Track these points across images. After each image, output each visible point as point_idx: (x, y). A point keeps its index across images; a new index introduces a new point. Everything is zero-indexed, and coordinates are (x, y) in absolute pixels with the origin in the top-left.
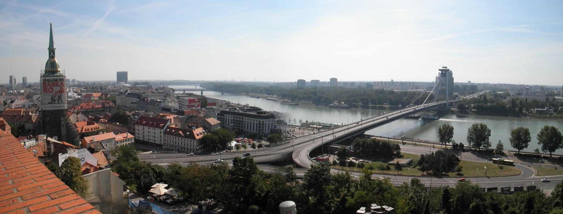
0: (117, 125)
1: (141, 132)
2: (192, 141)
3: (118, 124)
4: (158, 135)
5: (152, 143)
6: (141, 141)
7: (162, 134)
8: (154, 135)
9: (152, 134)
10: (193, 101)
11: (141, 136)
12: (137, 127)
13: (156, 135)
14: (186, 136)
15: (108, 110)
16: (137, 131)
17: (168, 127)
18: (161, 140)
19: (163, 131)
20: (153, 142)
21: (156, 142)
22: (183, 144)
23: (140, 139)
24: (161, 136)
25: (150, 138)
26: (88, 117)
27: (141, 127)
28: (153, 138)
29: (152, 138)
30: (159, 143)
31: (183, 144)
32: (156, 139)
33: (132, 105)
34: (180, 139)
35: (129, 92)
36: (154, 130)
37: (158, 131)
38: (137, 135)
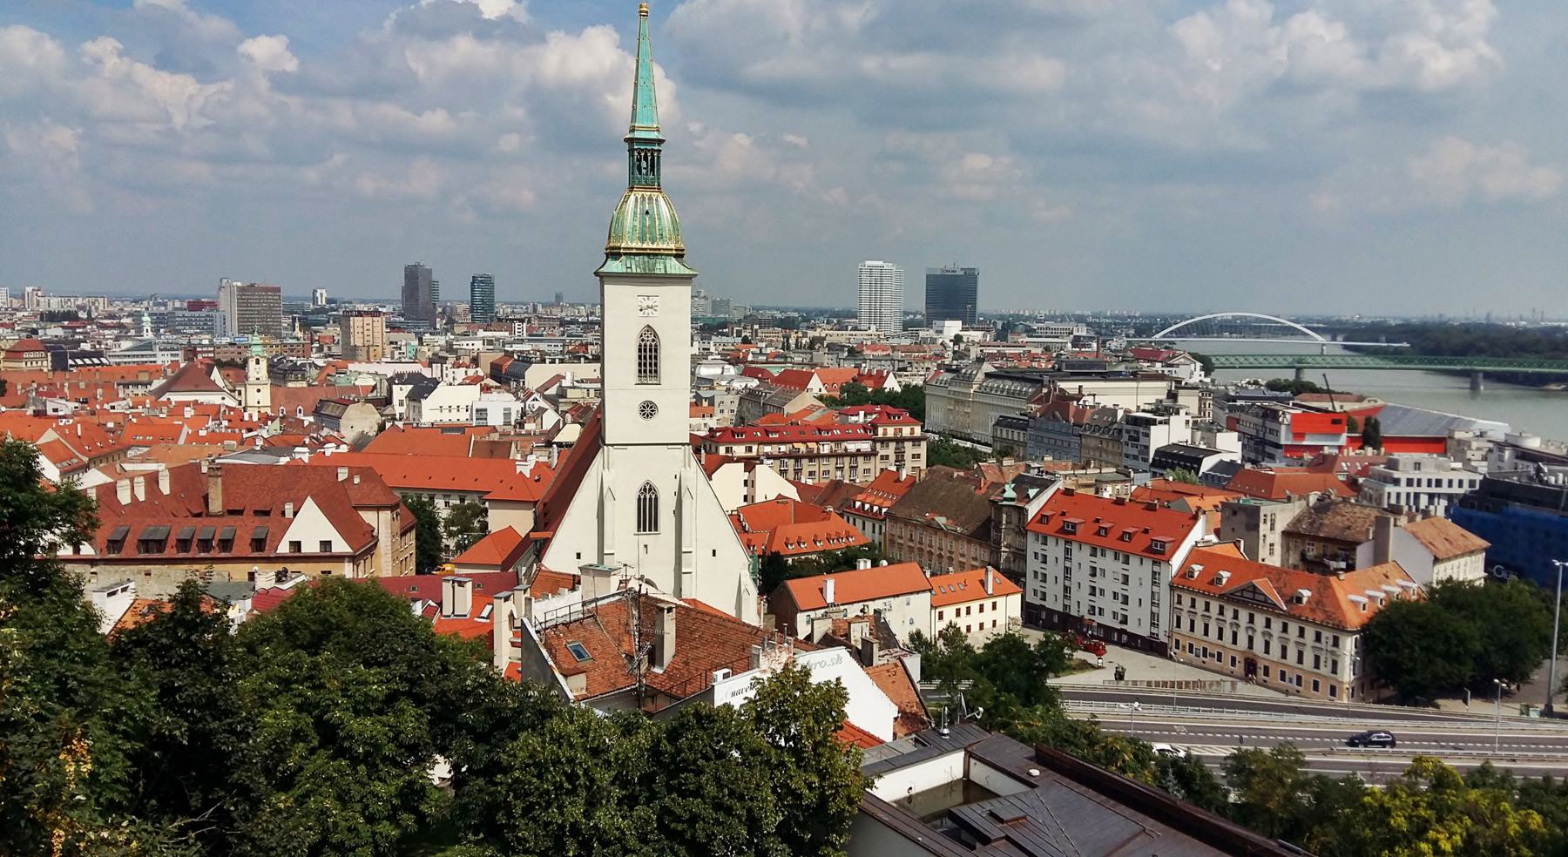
1: (1054, 570)
2: (1327, 635)
3: (941, 520)
4: (1139, 589)
6: (1051, 612)
8: (1118, 587)
9: (1109, 584)
12: (1033, 546)
13: (1133, 591)
15: (891, 450)
16: (1032, 565)
17: (1196, 554)
21: (1131, 627)
23: (1049, 604)
25: (1099, 602)
26: (796, 483)
27: (1055, 550)
28: (1117, 606)
29: (1109, 604)
30: (1144, 631)
32: (1133, 611)
33: (1004, 433)
34: (1260, 620)
35: (987, 367)
36: (1119, 565)
37: (1140, 570)
38: (1032, 583)
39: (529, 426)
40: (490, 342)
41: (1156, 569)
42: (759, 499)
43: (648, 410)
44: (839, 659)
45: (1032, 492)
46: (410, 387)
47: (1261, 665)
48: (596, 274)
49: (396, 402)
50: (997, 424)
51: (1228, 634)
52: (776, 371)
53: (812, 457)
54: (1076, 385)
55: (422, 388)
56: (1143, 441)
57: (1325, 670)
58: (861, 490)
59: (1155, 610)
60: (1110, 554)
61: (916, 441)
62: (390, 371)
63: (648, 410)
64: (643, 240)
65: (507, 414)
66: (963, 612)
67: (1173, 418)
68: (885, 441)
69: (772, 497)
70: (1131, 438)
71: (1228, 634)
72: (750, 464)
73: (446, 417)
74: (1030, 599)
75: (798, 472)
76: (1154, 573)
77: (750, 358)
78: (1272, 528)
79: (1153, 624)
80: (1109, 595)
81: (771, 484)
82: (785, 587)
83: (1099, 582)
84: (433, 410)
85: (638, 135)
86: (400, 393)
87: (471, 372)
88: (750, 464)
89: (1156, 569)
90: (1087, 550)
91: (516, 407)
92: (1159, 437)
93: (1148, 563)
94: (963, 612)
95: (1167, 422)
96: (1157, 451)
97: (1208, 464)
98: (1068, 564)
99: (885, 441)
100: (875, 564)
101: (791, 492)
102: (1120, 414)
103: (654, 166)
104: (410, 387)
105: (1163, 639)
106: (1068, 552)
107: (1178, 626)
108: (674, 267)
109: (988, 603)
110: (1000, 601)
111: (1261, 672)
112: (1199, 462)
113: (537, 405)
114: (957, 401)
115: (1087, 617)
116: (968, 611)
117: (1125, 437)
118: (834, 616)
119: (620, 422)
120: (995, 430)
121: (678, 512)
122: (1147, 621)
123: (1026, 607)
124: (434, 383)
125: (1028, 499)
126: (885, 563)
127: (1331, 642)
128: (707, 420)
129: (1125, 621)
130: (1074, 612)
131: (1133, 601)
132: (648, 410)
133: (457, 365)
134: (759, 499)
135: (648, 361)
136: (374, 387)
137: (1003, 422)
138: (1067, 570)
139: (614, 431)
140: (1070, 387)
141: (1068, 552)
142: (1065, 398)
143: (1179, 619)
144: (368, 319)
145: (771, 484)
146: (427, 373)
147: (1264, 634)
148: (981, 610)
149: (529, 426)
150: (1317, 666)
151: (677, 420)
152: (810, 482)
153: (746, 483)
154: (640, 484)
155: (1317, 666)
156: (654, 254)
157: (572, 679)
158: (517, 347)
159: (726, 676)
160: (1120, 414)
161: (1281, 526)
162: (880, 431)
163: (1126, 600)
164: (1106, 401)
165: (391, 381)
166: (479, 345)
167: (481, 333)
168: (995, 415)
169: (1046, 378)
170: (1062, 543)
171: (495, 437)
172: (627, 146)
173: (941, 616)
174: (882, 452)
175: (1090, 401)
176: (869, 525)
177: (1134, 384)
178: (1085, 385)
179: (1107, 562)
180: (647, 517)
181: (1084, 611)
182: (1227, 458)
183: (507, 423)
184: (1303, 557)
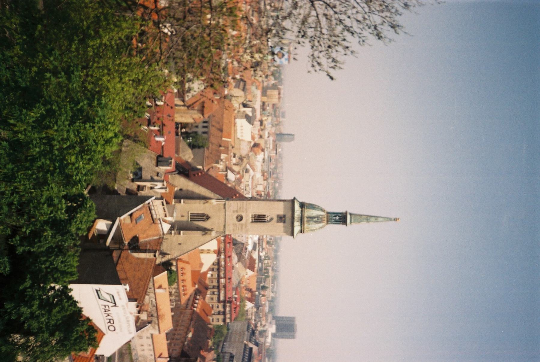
0: (187, 333)
3: (190, 335)
42: (202, 256)
44: (130, 333)
48: (295, 198)
50: (231, 354)
52: (255, 256)
58: (204, 299)
61: (224, 320)
68: (224, 307)
69: (203, 261)
82: (164, 271)
85: (349, 217)
99: (224, 307)
101: (204, 269)
103: (337, 222)
108: (297, 229)
134: (202, 256)
135: (259, 219)
139: (233, 205)
168: (234, 354)
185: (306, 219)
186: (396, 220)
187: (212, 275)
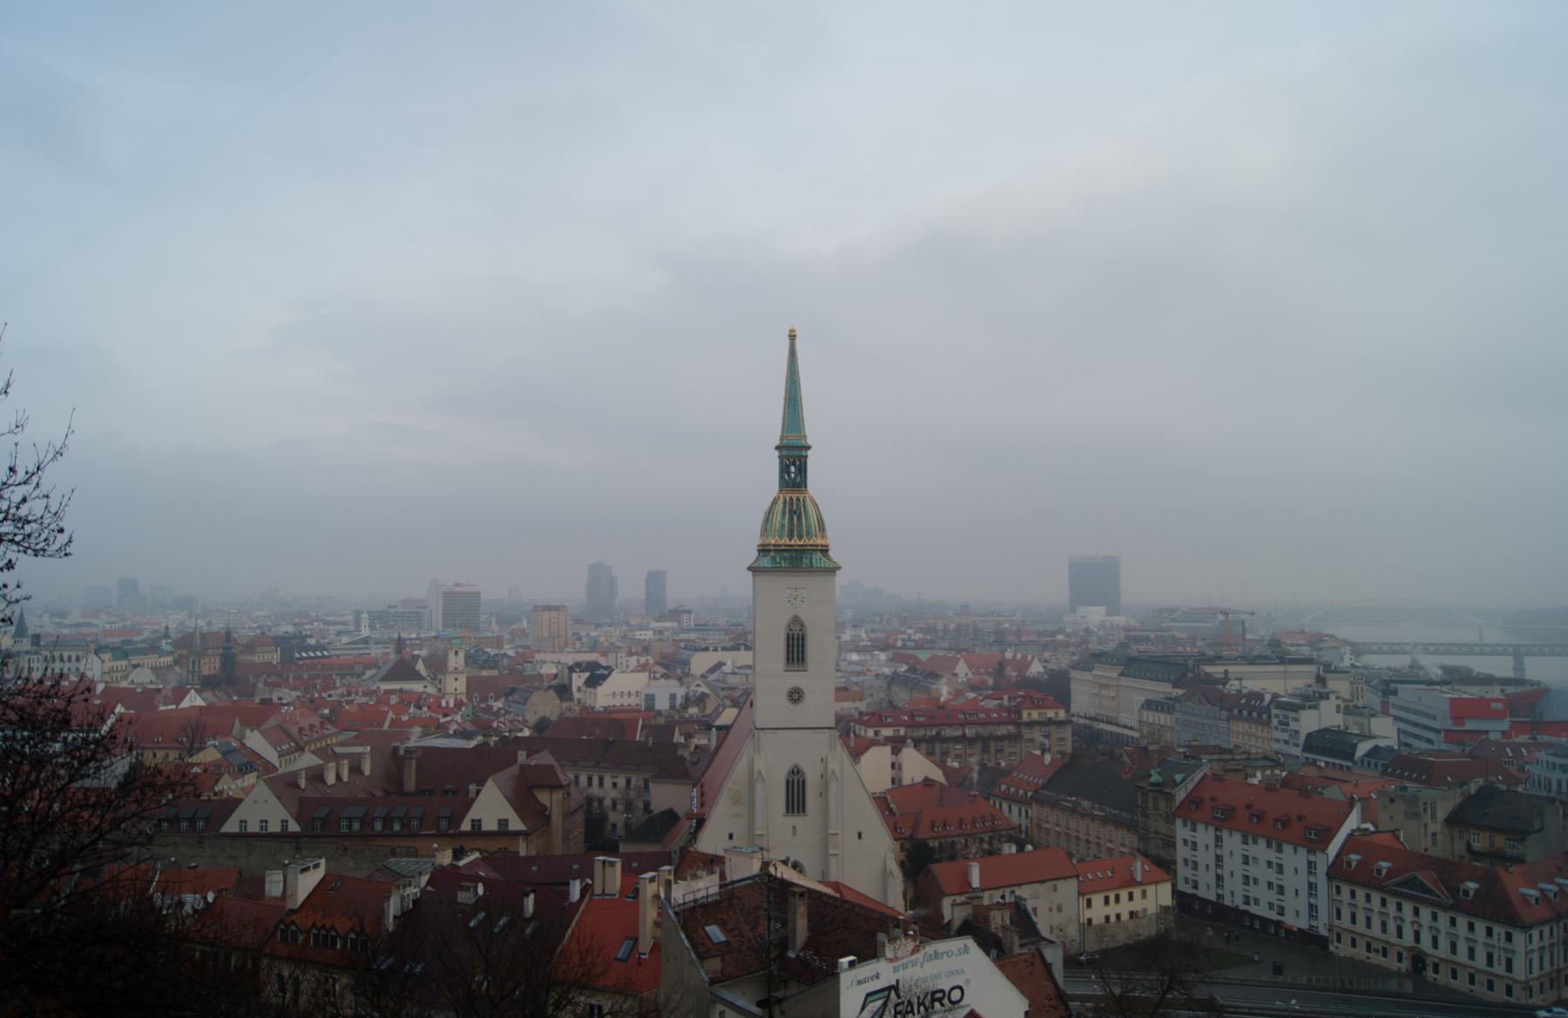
1: (1205, 857)
2: (1499, 930)
3: (1086, 804)
4: (1295, 880)
5: (1265, 922)
7: (1321, 880)
9: (1260, 871)
10: (1480, 708)
11: (1206, 879)
12: (1181, 832)
13: (1288, 880)
14: (1459, 905)
16: (1182, 852)
17: (1351, 843)
18: (1313, 908)
19: (1323, 861)
20: (1273, 916)
21: (1290, 920)
22: (1444, 942)
23: (1202, 893)
24: (1312, 887)
25: (1253, 892)
26: (942, 765)
27: (1205, 835)
28: (1273, 896)
30: (1302, 923)
31: (1444, 942)
33: (1150, 716)
34: (1425, 913)
37: (1295, 859)
38: (1182, 871)
39: (693, 710)
40: (661, 632)
41: (1312, 858)
42: (906, 781)
43: (796, 696)
44: (966, 949)
45: (1178, 777)
46: (587, 674)
47: (1429, 961)
48: (749, 568)
49: (574, 689)
51: (1392, 928)
53: (956, 740)
54: (1221, 669)
55: (597, 676)
56: (1293, 726)
57: (1499, 969)
59: (1313, 901)
60: (1262, 842)
62: (570, 659)
63: (796, 696)
64: (791, 537)
65: (673, 697)
66: (1112, 899)
67: (1323, 703)
69: (919, 779)
70: (1280, 722)
71: (1392, 928)
72: (897, 745)
73: (618, 702)
74: (1182, 887)
75: (945, 754)
76: (1310, 863)
77: (899, 644)
78: (1433, 817)
79: (1311, 916)
80: (1263, 884)
81: (917, 766)
83: (1253, 871)
84: (604, 697)
86: (578, 680)
87: (643, 660)
88: (897, 745)
89: (1312, 858)
90: (1237, 837)
91: (681, 692)
92: (1308, 722)
93: (1302, 852)
94: (1112, 899)
95: (1314, 707)
96: (1309, 736)
97: (1363, 748)
98: (1219, 852)
100: (1021, 849)
101: (937, 775)
102: (1268, 698)
104: (587, 674)
105: (1323, 932)
106: (1218, 839)
107: (1339, 917)
109: (1137, 892)
110: (1150, 889)
111: (1430, 969)
112: (1354, 746)
113: (700, 690)
114: (1102, 686)
115: (1243, 907)
116: (1117, 899)
117: (1275, 722)
118: (975, 902)
119: (770, 705)
120: (1140, 714)
121: (824, 794)
122: (1304, 911)
123: (1176, 893)
124: (610, 670)
125: (1175, 784)
126: (1029, 847)
127: (1503, 937)
128: (857, 704)
129: (1281, 911)
130: (1227, 902)
131: (1289, 891)
132: (796, 696)
133: (630, 654)
134: (906, 781)
136: (556, 676)
137: (1149, 705)
138: (1219, 858)
140: (1215, 670)
141: (1218, 839)
142: (1209, 680)
143: (1339, 911)
144: (554, 614)
145: (917, 766)
146: (602, 661)
147: (1430, 928)
148: (1131, 897)
149: (693, 710)
150: (1490, 963)
151: (822, 706)
152: (956, 765)
153: (893, 766)
154: (787, 767)
155: (1490, 963)
156: (801, 551)
157: (706, 963)
158: (682, 636)
159: (852, 964)
160: (1268, 698)
161: (1442, 814)
162: (1025, 715)
163: (1281, 890)
164: (1251, 685)
165: (571, 669)
166: (650, 635)
167: (653, 624)
168: (1143, 699)
169: (1190, 662)
170: (1211, 830)
171: (662, 721)
172: (777, 453)
173: (1089, 904)
174: (1027, 736)
175: (1234, 685)
176: (1015, 808)
177: (1280, 668)
178: (1231, 669)
179: (1260, 850)
180: (795, 800)
181: (1238, 902)
182: (1382, 743)
183: (672, 707)
184: (1469, 847)
185: (795, 541)
186: (792, 337)
187: (958, 756)
